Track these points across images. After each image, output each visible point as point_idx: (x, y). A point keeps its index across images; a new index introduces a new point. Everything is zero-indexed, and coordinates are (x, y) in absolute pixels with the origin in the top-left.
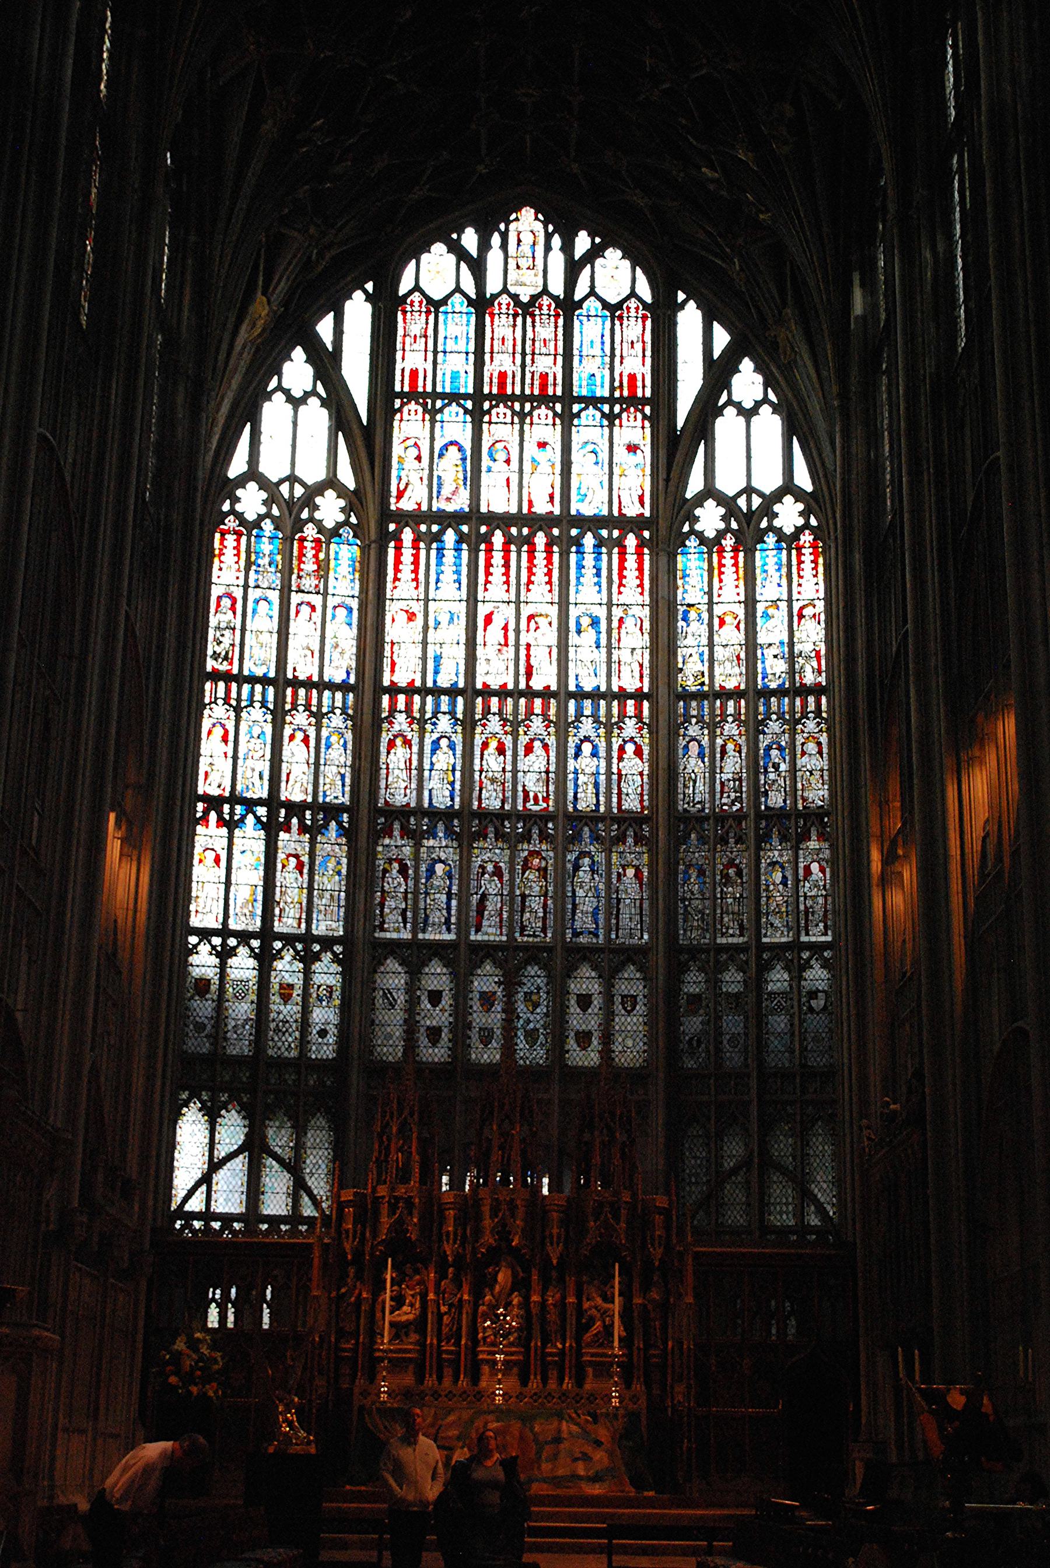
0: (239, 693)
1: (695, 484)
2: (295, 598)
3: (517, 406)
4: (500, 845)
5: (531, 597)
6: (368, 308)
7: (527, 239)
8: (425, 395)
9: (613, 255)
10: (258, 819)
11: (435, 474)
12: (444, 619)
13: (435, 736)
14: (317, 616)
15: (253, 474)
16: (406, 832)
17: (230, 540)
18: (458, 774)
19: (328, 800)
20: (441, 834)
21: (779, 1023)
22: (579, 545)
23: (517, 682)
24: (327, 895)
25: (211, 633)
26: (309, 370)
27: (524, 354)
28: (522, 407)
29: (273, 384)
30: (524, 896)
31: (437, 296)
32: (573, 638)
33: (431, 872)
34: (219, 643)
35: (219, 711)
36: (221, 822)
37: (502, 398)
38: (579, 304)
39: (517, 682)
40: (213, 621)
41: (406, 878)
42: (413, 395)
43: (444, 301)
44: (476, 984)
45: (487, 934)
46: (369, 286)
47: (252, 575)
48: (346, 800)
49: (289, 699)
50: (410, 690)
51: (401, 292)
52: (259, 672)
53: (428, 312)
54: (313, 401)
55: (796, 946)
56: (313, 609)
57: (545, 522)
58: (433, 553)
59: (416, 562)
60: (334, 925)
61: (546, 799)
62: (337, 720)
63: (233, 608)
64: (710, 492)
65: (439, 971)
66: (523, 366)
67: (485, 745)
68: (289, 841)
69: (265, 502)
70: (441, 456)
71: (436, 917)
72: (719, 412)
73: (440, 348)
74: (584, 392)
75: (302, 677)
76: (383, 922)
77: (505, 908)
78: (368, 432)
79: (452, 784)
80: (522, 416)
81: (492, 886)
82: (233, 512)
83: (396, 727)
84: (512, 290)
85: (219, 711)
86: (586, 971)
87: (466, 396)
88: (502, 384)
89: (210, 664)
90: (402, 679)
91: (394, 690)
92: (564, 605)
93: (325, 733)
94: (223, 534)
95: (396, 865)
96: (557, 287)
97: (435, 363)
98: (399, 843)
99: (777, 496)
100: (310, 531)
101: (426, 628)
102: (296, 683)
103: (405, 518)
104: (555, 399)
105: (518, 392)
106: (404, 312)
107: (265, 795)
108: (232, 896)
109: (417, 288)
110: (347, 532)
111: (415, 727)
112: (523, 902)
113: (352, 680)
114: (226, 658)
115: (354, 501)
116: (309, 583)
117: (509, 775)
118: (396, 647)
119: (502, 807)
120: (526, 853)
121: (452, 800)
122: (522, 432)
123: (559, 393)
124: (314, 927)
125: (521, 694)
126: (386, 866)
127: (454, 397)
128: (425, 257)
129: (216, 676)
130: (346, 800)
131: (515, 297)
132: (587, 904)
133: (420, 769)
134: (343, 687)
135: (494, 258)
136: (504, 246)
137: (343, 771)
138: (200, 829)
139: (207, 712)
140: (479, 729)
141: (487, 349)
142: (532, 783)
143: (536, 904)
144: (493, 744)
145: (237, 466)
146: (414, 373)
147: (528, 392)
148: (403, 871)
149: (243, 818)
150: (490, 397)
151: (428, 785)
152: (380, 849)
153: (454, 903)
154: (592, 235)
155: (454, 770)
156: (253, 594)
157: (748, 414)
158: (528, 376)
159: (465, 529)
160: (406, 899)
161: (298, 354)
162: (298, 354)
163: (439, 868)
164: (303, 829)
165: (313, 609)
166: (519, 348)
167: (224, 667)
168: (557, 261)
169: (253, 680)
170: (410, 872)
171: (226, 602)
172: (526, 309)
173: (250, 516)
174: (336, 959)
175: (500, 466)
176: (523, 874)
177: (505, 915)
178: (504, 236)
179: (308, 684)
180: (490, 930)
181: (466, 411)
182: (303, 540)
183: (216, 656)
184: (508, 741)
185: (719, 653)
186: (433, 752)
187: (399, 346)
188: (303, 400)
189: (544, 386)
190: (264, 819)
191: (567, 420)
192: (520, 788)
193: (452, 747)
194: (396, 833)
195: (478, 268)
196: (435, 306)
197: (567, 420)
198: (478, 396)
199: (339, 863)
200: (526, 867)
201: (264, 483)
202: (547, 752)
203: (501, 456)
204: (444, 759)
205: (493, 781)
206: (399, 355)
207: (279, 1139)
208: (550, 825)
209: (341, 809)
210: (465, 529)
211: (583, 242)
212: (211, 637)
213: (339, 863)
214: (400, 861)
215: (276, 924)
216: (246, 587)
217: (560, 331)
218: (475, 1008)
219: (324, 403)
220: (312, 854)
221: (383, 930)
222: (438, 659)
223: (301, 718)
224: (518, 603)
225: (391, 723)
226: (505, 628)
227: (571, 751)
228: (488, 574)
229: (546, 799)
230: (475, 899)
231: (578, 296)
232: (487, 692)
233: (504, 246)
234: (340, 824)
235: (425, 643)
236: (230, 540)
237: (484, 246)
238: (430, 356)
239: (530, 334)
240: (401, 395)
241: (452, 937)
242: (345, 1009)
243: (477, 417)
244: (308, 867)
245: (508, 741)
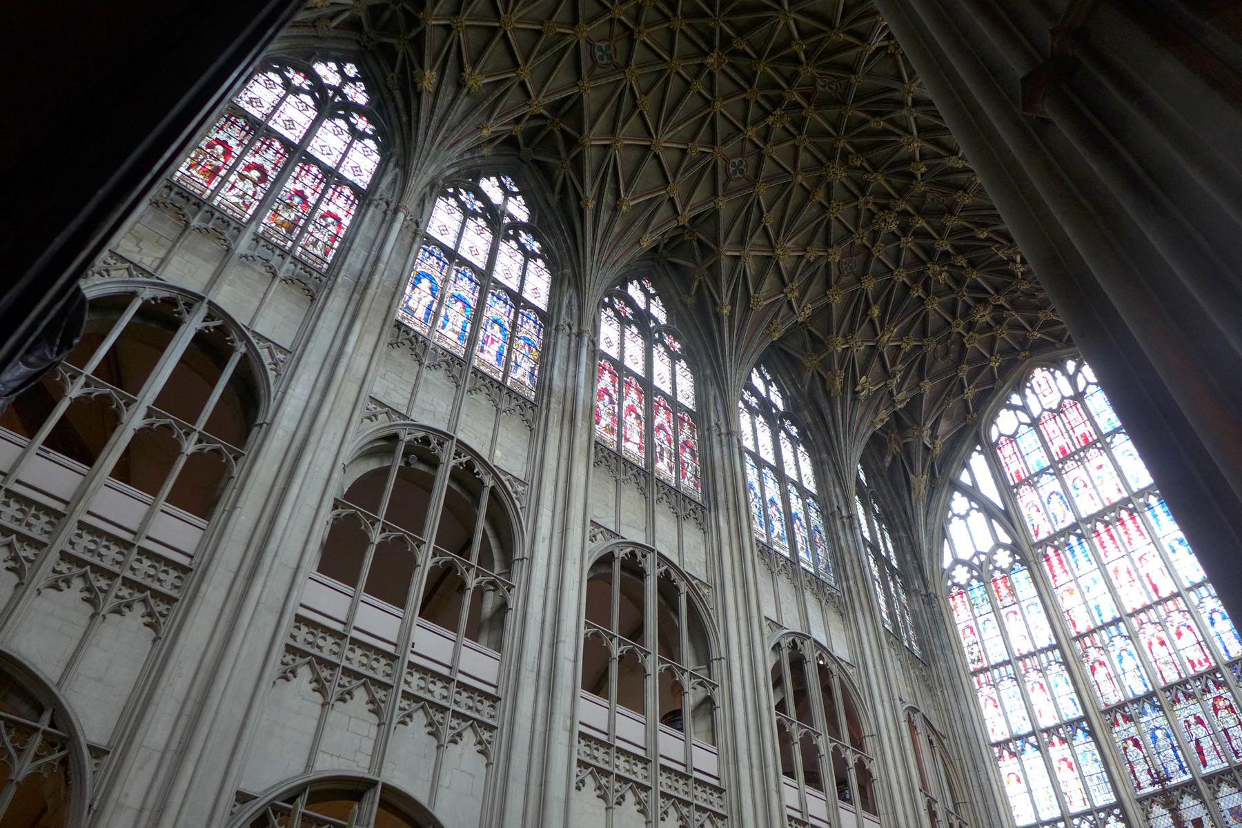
0: (993, 677)
2: (1003, 612)
3: (1076, 457)
4: (1191, 702)
5: (1134, 547)
6: (982, 457)
7: (1043, 382)
8: (1027, 480)
10: (1033, 745)
11: (1050, 513)
12: (1090, 584)
13: (1117, 652)
14: (1019, 616)
15: (957, 561)
16: (1128, 719)
17: (958, 598)
18: (1142, 669)
19: (1070, 717)
20: (1149, 711)
22: (1148, 505)
23: (1150, 598)
24: (1094, 777)
25: (966, 650)
26: (965, 499)
27: (1067, 431)
28: (1079, 456)
29: (950, 514)
30: (1225, 730)
31: (1011, 432)
32: (1172, 556)
33: (1154, 738)
34: (972, 653)
35: (986, 690)
36: (1012, 754)
37: (1067, 457)
38: (1084, 393)
39: (1150, 598)
40: (965, 644)
41: (1140, 749)
42: (1022, 482)
43: (1016, 432)
44: (1222, 804)
45: (1212, 766)
46: (978, 448)
47: (976, 611)
48: (1081, 713)
49: (1022, 668)
50: (1091, 632)
51: (994, 440)
52: (1000, 660)
53: (1011, 442)
54: (973, 513)
56: (1015, 613)
57: (1123, 504)
58: (1068, 553)
59: (1061, 562)
60: (1108, 796)
61: (1207, 660)
62: (1055, 668)
63: (972, 631)
65: (1192, 804)
66: (1070, 437)
67: (1150, 644)
68: (1058, 751)
69: (968, 572)
70: (1049, 502)
71: (1173, 766)
73: (1024, 454)
74: (1109, 429)
75: (1025, 652)
76: (1139, 784)
77: (1216, 743)
78: (1006, 513)
79: (1141, 676)
80: (1080, 460)
81: (1199, 731)
82: (954, 584)
83: (1092, 658)
84: (1047, 407)
85: (986, 690)
87: (1048, 468)
88: (1064, 452)
89: (972, 667)
90: (1082, 628)
91: (1080, 637)
92: (1155, 542)
93: (1051, 678)
94: (953, 598)
95: (1130, 742)
96: (1069, 392)
97: (1025, 463)
98: (1125, 727)
100: (997, 575)
101: (1082, 594)
102: (1022, 658)
103: (1042, 543)
104: (1095, 442)
105: (1073, 450)
106: (1000, 449)
107: (1030, 729)
108: (1035, 798)
109: (1001, 435)
110: (1017, 566)
111: (1102, 652)
112: (1227, 734)
113: (1054, 642)
114: (979, 660)
115: (1015, 548)
116: (1008, 601)
117: (1174, 656)
118: (1070, 612)
119: (1181, 677)
120: (1211, 701)
121: (1146, 685)
122: (1085, 468)
123: (1095, 437)
124: (1095, 801)
125: (1157, 603)
126: (1125, 745)
127: (1043, 471)
128: (999, 421)
129: (976, 673)
130: (1081, 713)
131: (1050, 410)
133: (1117, 676)
134: (1051, 648)
135: (1032, 400)
136: (1033, 392)
137: (1071, 696)
138: (1001, 763)
139: (979, 694)
140: (1141, 636)
141: (1048, 440)
144: (1155, 642)
145: (947, 561)
146: (1018, 472)
147: (1078, 447)
148: (1136, 744)
149: (1023, 750)
150: (1061, 461)
151: (1126, 684)
152: (1115, 735)
153: (1179, 753)
154: (1073, 358)
155: (1138, 667)
156: (980, 620)
158: (1075, 440)
159: (1079, 531)
160: (1146, 762)
161: (957, 495)
162: (957, 495)
163: (1159, 733)
164: (1063, 740)
165: (1015, 613)
166: (1064, 431)
167: (979, 666)
168: (1063, 381)
169: (997, 666)
170: (1141, 743)
171: (968, 631)
172: (1059, 411)
173: (963, 582)
174: (1119, 820)
175: (1082, 490)
176: (1217, 715)
177: (1219, 748)
178: (1031, 388)
179: (1031, 655)
180: (1214, 762)
181: (1051, 474)
182: (995, 581)
183: (973, 662)
184: (1163, 635)
186: (1121, 661)
187: (1004, 465)
188: (968, 514)
189: (1086, 440)
190: (1036, 744)
191: (1107, 448)
192: (1186, 660)
193: (1130, 654)
194: (1121, 721)
195: (1025, 408)
196: (1012, 438)
197: (1107, 448)
198: (1053, 464)
199: (1093, 754)
200: (1216, 710)
201: (964, 563)
202: (1191, 630)
203: (1079, 484)
204: (1130, 663)
205: (1166, 663)
206: (1006, 469)
208: (1218, 675)
209: (1079, 720)
210: (1079, 531)
212: (966, 653)
213: (1093, 754)
214: (1132, 739)
215: (1070, 807)
216: (975, 618)
217: (1081, 410)
218: (1231, 822)
219: (978, 510)
220: (1074, 755)
221: (1140, 788)
222: (1097, 608)
223: (1033, 676)
224: (1128, 554)
225: (1087, 656)
226: (1129, 572)
227: (1208, 623)
228: (1104, 547)
229: (1207, 660)
230: (1193, 744)
231: (1081, 389)
232: (1136, 613)
233: (1033, 392)
234: (1083, 730)
235: (1085, 603)
236: (958, 598)
237: (1024, 397)
238: (1021, 460)
239: (1066, 421)
240: (1017, 486)
241: (1189, 776)
243: (1058, 474)
244: (1073, 765)
245: (1163, 635)
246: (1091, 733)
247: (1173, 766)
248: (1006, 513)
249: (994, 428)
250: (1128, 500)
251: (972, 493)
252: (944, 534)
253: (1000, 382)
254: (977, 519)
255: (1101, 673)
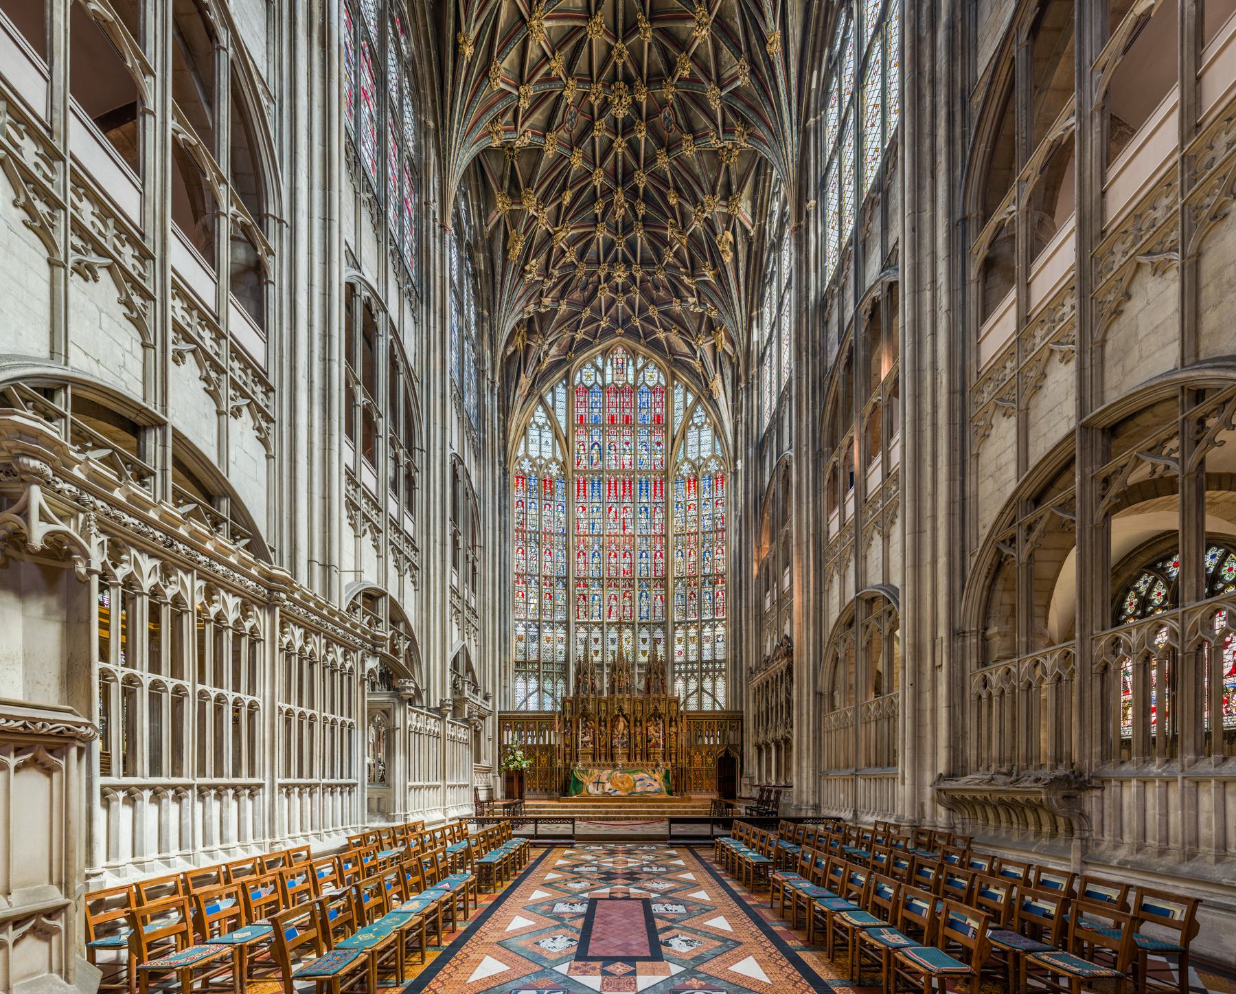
1: (681, 456)
9: (651, 367)
21: (707, 646)
55: (713, 620)
64: (686, 459)
72: (689, 428)
81: (613, 603)
86: (644, 630)
96: (631, 382)
99: (709, 459)
132: (645, 609)
135: (609, 370)
142: (625, 567)
143: (628, 609)
145: (520, 453)
154: (644, 358)
157: (699, 428)
161: (540, 408)
168: (631, 371)
185: (689, 519)
195: (603, 372)
207: (548, 686)
211: (640, 363)
237: (605, 364)
242: (568, 644)
246: (566, 586)
247: (596, 614)
248: (566, 439)
249: (578, 375)
250: (633, 473)
251: (550, 413)
252: (525, 433)
253: (597, 341)
254: (548, 436)
255: (582, 557)
